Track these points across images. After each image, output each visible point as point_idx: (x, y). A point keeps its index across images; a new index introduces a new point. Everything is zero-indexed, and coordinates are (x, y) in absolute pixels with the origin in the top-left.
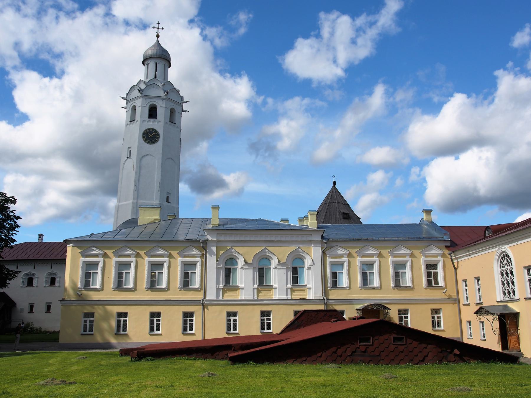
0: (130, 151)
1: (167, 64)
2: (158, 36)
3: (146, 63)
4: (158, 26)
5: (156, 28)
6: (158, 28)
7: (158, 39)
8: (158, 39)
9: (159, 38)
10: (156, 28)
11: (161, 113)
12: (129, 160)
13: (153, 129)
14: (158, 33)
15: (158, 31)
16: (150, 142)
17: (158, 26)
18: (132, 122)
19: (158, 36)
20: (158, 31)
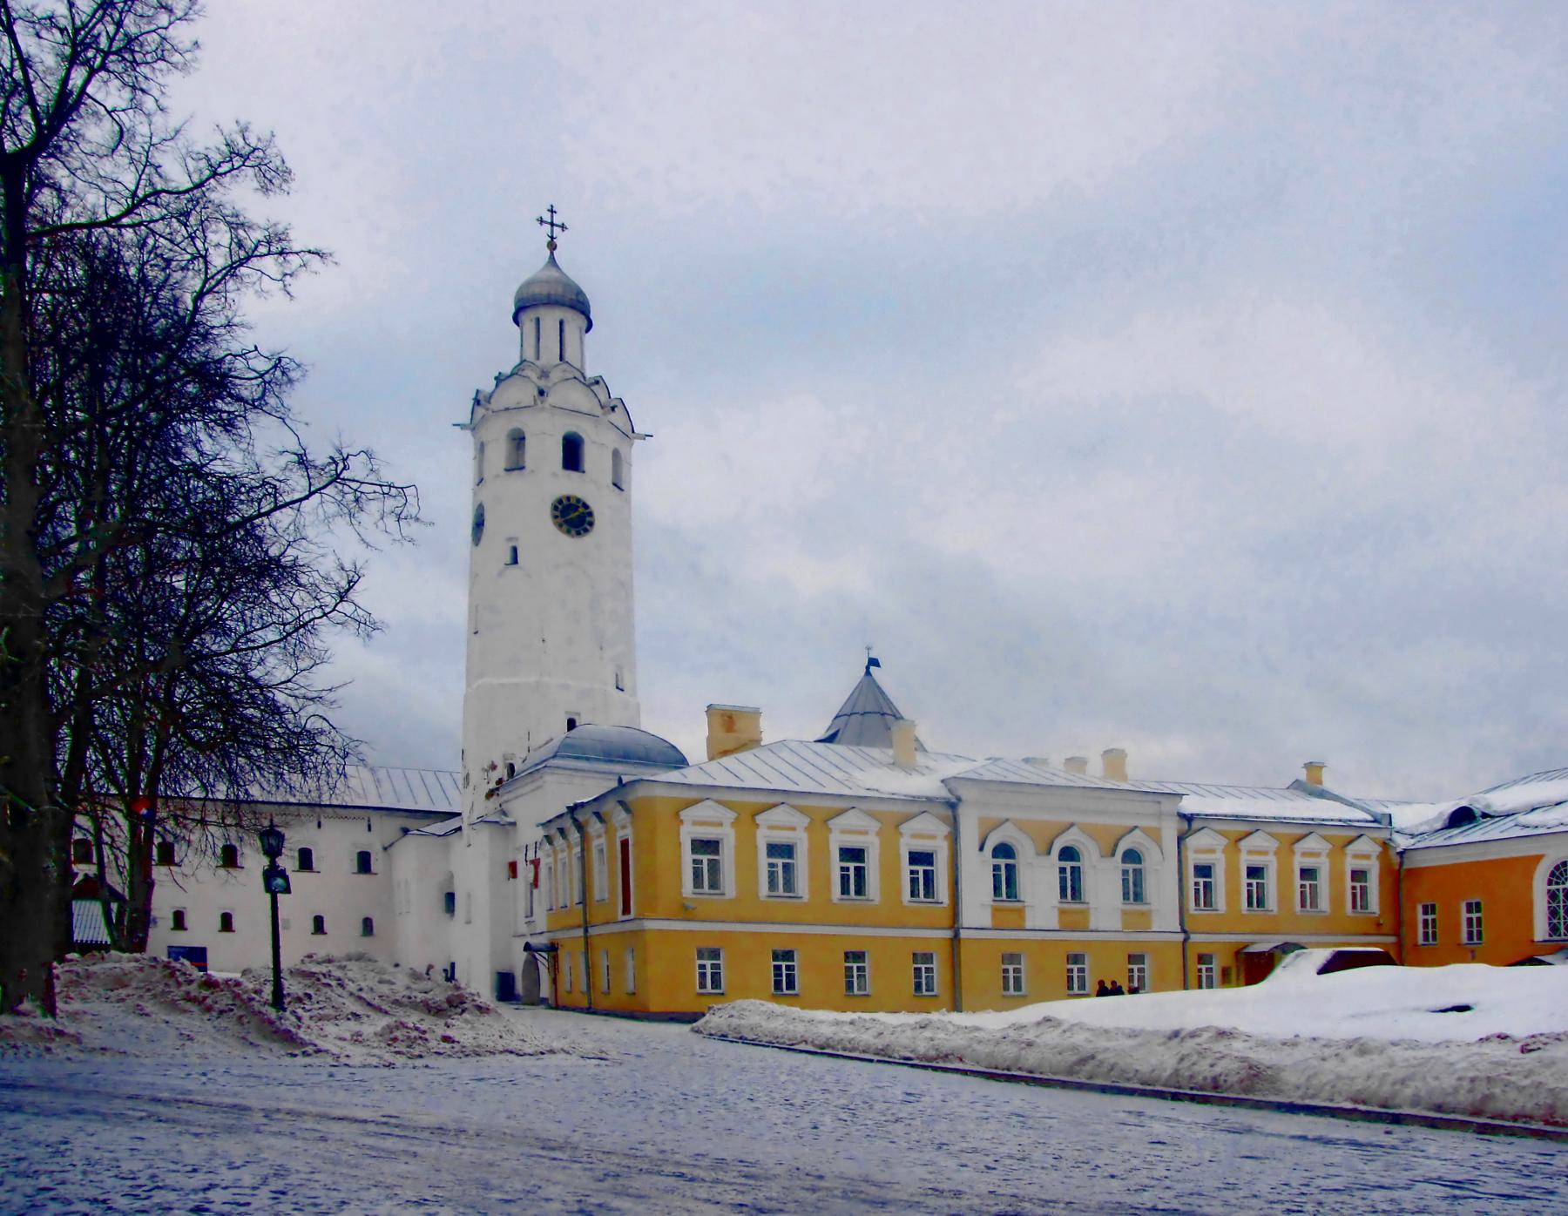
0: (515, 550)
1: (585, 325)
2: (552, 246)
3: (528, 318)
4: (552, 217)
5: (546, 222)
6: (552, 224)
7: (552, 253)
8: (552, 253)
9: (555, 252)
10: (546, 222)
11: (590, 455)
12: (514, 570)
13: (578, 500)
14: (552, 238)
15: (552, 231)
16: (573, 532)
17: (552, 217)
18: (516, 472)
19: (552, 246)
20: (552, 231)
